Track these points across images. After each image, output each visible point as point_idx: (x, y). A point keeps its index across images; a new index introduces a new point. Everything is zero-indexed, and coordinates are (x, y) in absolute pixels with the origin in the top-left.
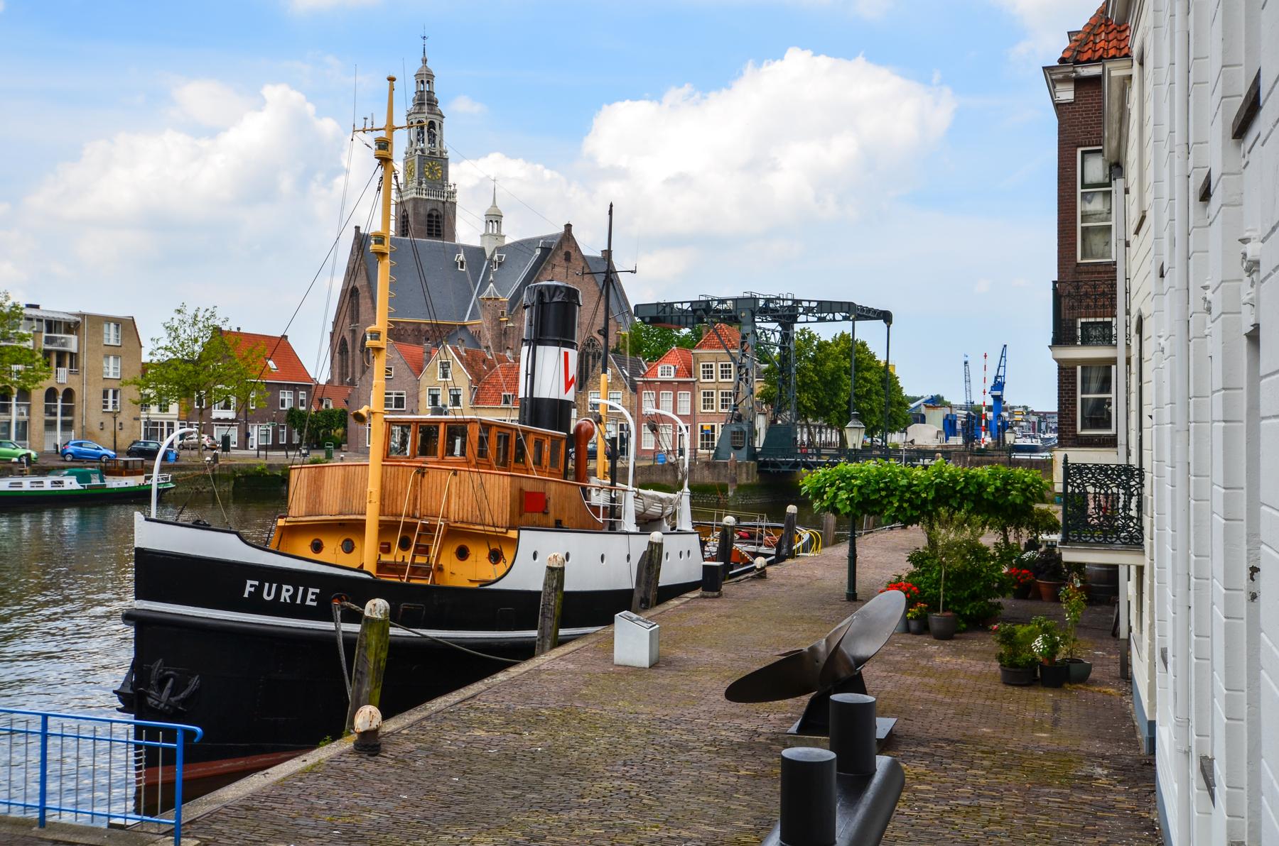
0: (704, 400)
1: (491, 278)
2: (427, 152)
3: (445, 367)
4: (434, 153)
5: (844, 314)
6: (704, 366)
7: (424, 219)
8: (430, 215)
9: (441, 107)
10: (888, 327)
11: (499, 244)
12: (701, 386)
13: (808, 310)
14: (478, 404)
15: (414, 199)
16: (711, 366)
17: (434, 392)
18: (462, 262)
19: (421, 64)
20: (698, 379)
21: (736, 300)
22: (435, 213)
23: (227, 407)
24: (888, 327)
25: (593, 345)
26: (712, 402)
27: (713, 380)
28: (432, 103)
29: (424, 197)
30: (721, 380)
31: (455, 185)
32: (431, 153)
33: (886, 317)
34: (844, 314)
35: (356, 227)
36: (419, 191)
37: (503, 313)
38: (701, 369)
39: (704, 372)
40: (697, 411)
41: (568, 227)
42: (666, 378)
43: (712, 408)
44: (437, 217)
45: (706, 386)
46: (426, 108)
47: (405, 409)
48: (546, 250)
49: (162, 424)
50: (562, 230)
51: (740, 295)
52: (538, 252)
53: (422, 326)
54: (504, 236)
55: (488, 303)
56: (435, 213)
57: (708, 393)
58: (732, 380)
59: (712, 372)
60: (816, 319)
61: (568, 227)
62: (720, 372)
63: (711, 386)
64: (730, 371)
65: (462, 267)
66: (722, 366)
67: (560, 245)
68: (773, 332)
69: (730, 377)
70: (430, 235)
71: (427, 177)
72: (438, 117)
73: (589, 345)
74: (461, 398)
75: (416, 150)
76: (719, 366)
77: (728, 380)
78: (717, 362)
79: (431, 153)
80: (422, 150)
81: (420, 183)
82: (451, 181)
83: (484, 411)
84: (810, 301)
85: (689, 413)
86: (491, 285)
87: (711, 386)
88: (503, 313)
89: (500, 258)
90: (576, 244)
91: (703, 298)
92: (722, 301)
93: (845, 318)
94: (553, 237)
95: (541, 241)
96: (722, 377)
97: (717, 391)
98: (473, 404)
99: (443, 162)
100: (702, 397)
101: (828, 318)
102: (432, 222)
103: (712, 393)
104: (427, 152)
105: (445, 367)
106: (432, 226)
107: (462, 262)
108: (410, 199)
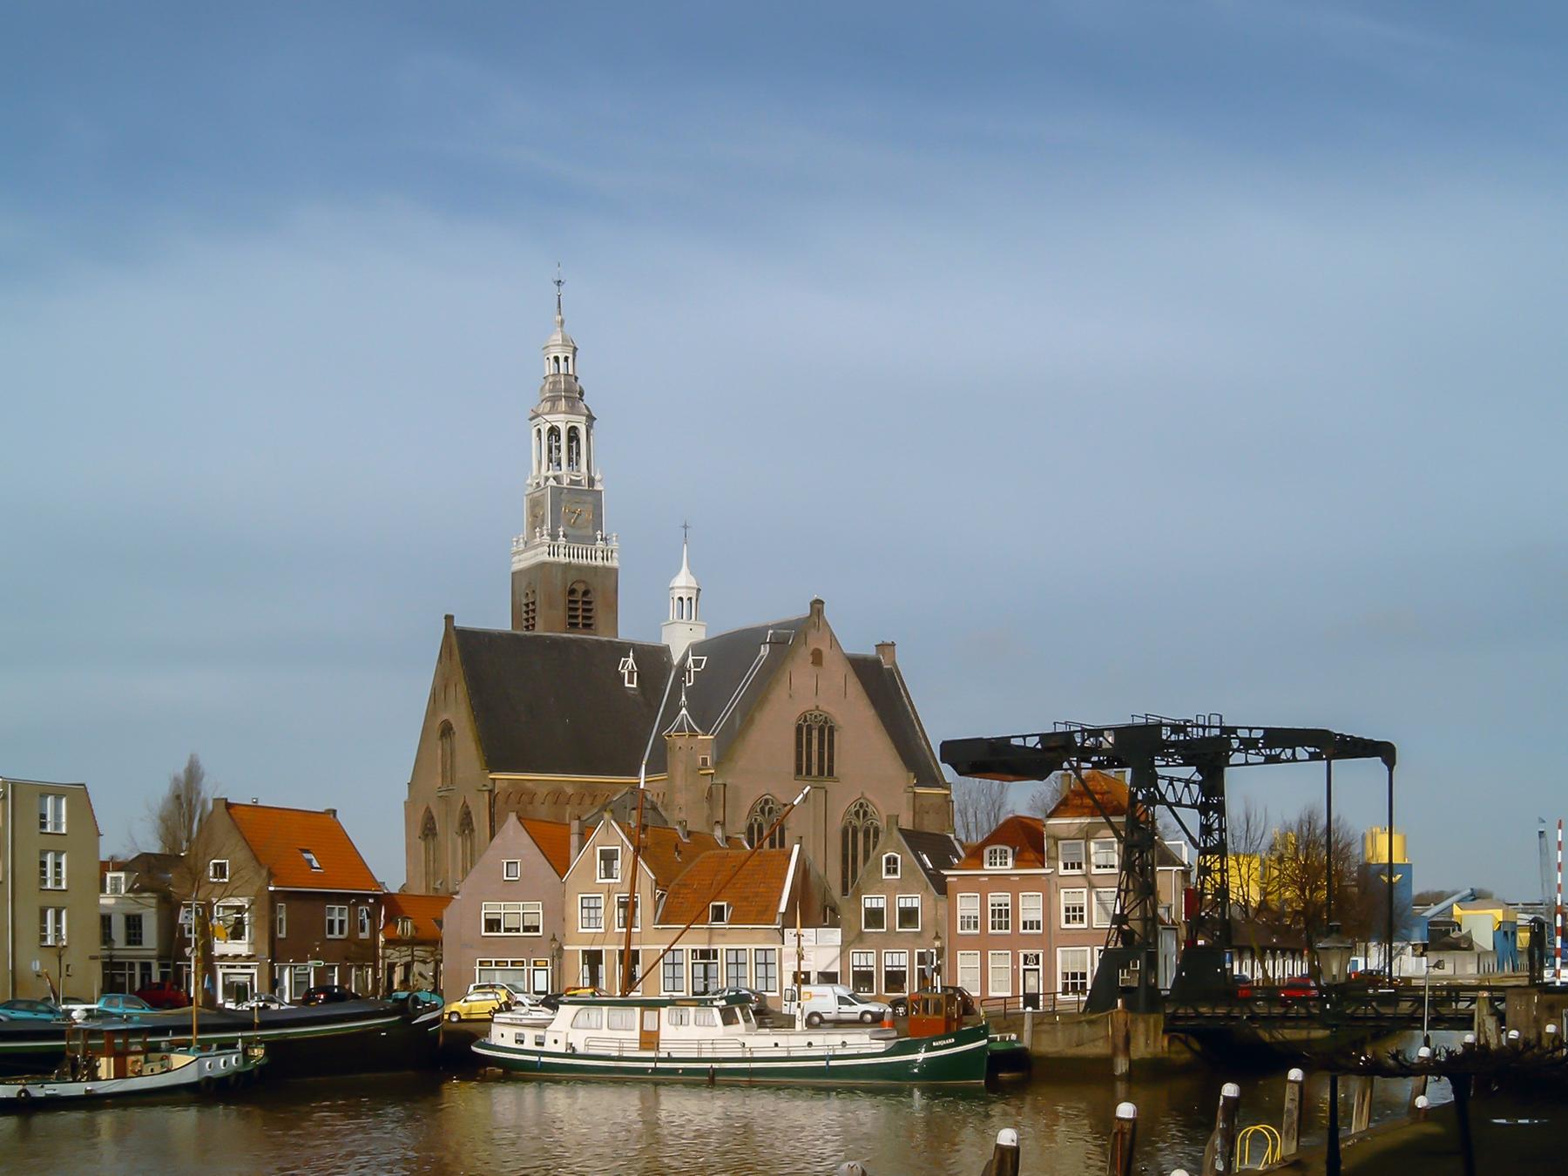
2: (566, 481)
3: (608, 857)
4: (578, 483)
5: (1312, 750)
7: (561, 600)
8: (572, 592)
12: (1060, 881)
13: (1249, 744)
21: (1119, 731)
22: (581, 588)
23: (237, 934)
29: (563, 559)
32: (572, 482)
33: (1386, 752)
34: (1312, 750)
37: (705, 760)
40: (1054, 928)
41: (817, 606)
49: (132, 965)
52: (765, 651)
56: (581, 588)
60: (1262, 759)
61: (817, 606)
68: (1187, 783)
73: (857, 813)
75: (547, 479)
84: (1251, 729)
88: (705, 760)
90: (832, 634)
91: (1061, 729)
92: (1097, 733)
93: (1313, 757)
95: (770, 632)
101: (1283, 756)
104: (566, 481)
105: (608, 857)
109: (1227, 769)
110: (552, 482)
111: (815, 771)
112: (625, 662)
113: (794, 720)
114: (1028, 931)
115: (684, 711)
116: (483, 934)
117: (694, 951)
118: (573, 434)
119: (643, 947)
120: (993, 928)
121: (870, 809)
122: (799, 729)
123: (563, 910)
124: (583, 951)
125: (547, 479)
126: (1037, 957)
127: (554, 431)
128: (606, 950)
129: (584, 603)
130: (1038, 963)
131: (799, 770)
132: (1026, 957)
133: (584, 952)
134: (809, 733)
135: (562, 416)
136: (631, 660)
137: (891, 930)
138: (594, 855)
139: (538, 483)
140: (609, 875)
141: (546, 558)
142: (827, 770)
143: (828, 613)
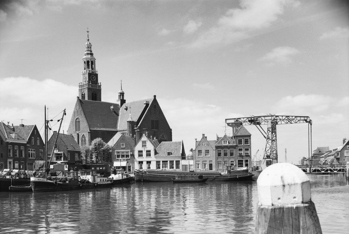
3: (144, 142)
8: (93, 94)
20: (237, 145)
22: (94, 93)
31: (100, 83)
35: (77, 97)
41: (155, 96)
47: (129, 158)
50: (153, 98)
56: (94, 93)
61: (155, 96)
78: (243, 139)
80: (89, 71)
82: (99, 82)
84: (292, 116)
87: (242, 147)
99: (96, 75)
105: (144, 142)
117: (163, 162)
126: (233, 161)
130: (233, 162)
132: (231, 161)
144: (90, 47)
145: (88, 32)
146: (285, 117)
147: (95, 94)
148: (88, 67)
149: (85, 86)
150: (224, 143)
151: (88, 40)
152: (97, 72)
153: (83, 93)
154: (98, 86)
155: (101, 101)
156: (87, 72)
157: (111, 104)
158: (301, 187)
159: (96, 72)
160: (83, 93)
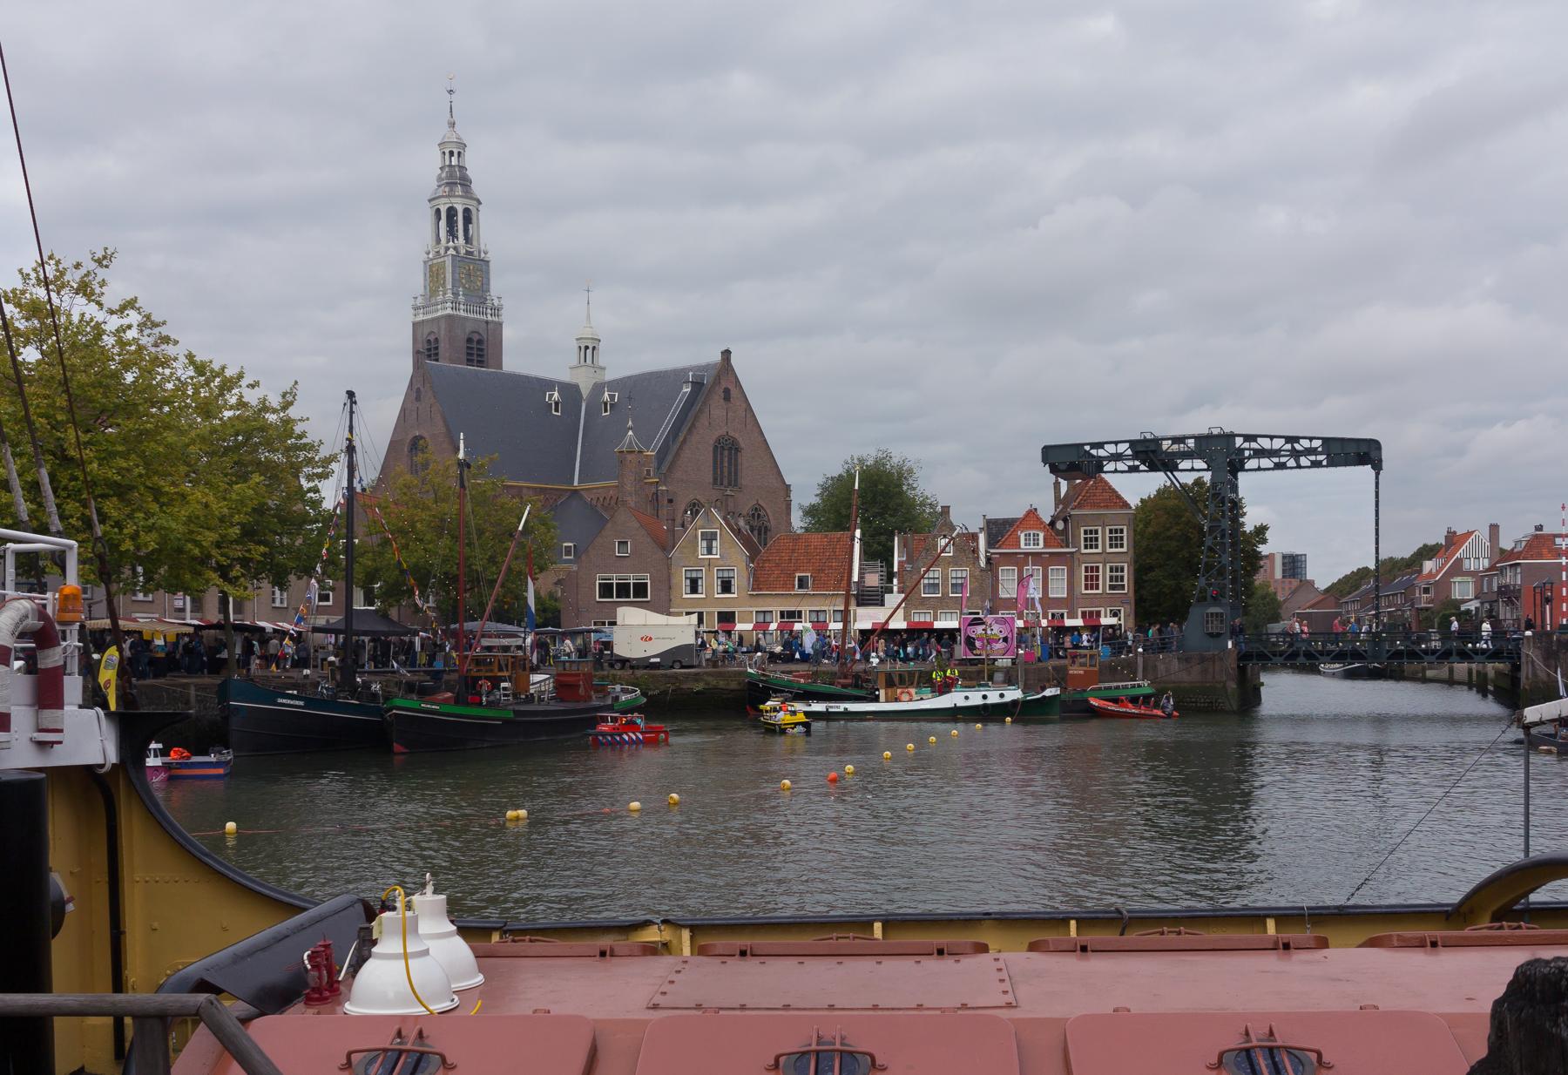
0: (1086, 577)
1: (630, 423)
2: (463, 251)
3: (710, 538)
6: (1086, 532)
7: (463, 345)
8: (469, 340)
9: (476, 188)
10: (1377, 475)
11: (598, 378)
12: (1081, 558)
14: (761, 589)
15: (449, 316)
16: (1096, 532)
17: (694, 575)
18: (557, 404)
19: (446, 129)
22: (476, 337)
24: (1377, 475)
25: (759, 515)
26: (1097, 579)
27: (1099, 550)
28: (465, 182)
29: (462, 313)
30: (1109, 550)
32: (468, 253)
36: (455, 302)
37: (648, 471)
38: (1082, 536)
39: (1086, 539)
41: (727, 354)
42: (1032, 548)
43: (1097, 588)
44: (480, 342)
45: (1086, 558)
46: (459, 190)
47: (649, 599)
48: (697, 385)
50: (716, 357)
51: (1137, 437)
52: (687, 389)
53: (525, 491)
54: (604, 369)
55: (629, 457)
56: (476, 337)
57: (1092, 567)
58: (1124, 550)
59: (1097, 539)
61: (727, 354)
62: (1108, 539)
63: (1097, 558)
64: (1122, 538)
65: (557, 410)
66: (1111, 531)
67: (717, 380)
69: (1122, 546)
70: (470, 362)
71: (464, 287)
72: (475, 203)
74: (735, 583)
75: (447, 249)
76: (1108, 531)
77: (1119, 550)
79: (468, 253)
80: (455, 248)
81: (456, 294)
83: (769, 600)
85: (1065, 596)
86: (630, 433)
87: (1097, 558)
88: (648, 471)
89: (612, 397)
90: (736, 377)
94: (707, 367)
95: (691, 374)
96: (1111, 546)
97: (1104, 566)
98: (753, 590)
100: (1083, 574)
102: (472, 348)
103: (1097, 568)
104: (463, 251)
105: (710, 538)
106: (478, 355)
107: (557, 404)
108: (442, 317)
109: (1240, 475)
110: (451, 252)
111: (725, 482)
112: (551, 396)
113: (712, 442)
114: (1089, 592)
115: (630, 433)
116: (598, 599)
117: (782, 613)
118: (467, 211)
119: (708, 610)
120: (1122, 587)
121: (762, 513)
122: (715, 452)
123: (669, 581)
124: (719, 613)
125: (447, 249)
127: (451, 212)
128: (707, 613)
129: (478, 349)
131: (715, 482)
133: (719, 613)
134: (722, 454)
135: (459, 200)
136: (556, 394)
137: (945, 595)
138: (696, 536)
139: (438, 252)
140: (710, 552)
141: (449, 311)
142: (734, 482)
143: (734, 361)
144: (459, 153)
145: (451, 92)
146: (1283, 441)
147: (480, 342)
148: (452, 232)
149: (439, 307)
150: (1026, 545)
151: (452, 125)
152: (486, 253)
153: (432, 338)
154: (489, 311)
155: (500, 367)
156: (449, 252)
157: (549, 385)
158: (1337, 711)
159: (483, 255)
160: (432, 338)
